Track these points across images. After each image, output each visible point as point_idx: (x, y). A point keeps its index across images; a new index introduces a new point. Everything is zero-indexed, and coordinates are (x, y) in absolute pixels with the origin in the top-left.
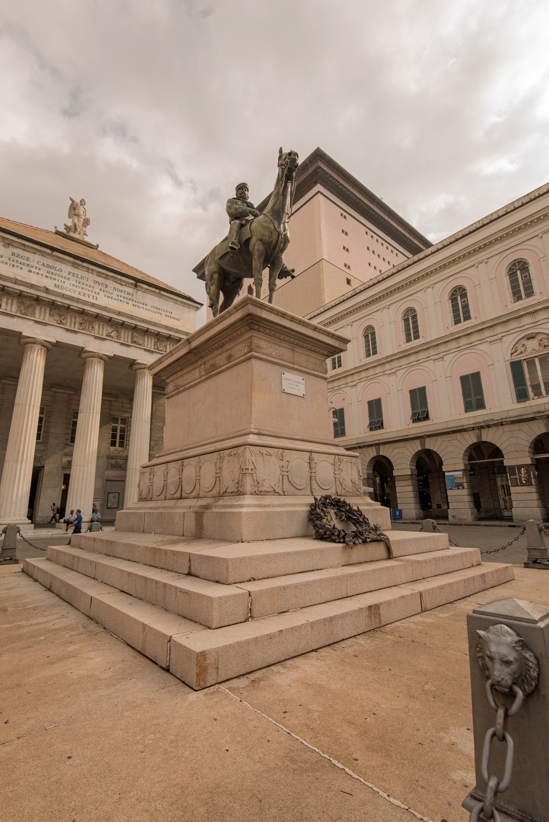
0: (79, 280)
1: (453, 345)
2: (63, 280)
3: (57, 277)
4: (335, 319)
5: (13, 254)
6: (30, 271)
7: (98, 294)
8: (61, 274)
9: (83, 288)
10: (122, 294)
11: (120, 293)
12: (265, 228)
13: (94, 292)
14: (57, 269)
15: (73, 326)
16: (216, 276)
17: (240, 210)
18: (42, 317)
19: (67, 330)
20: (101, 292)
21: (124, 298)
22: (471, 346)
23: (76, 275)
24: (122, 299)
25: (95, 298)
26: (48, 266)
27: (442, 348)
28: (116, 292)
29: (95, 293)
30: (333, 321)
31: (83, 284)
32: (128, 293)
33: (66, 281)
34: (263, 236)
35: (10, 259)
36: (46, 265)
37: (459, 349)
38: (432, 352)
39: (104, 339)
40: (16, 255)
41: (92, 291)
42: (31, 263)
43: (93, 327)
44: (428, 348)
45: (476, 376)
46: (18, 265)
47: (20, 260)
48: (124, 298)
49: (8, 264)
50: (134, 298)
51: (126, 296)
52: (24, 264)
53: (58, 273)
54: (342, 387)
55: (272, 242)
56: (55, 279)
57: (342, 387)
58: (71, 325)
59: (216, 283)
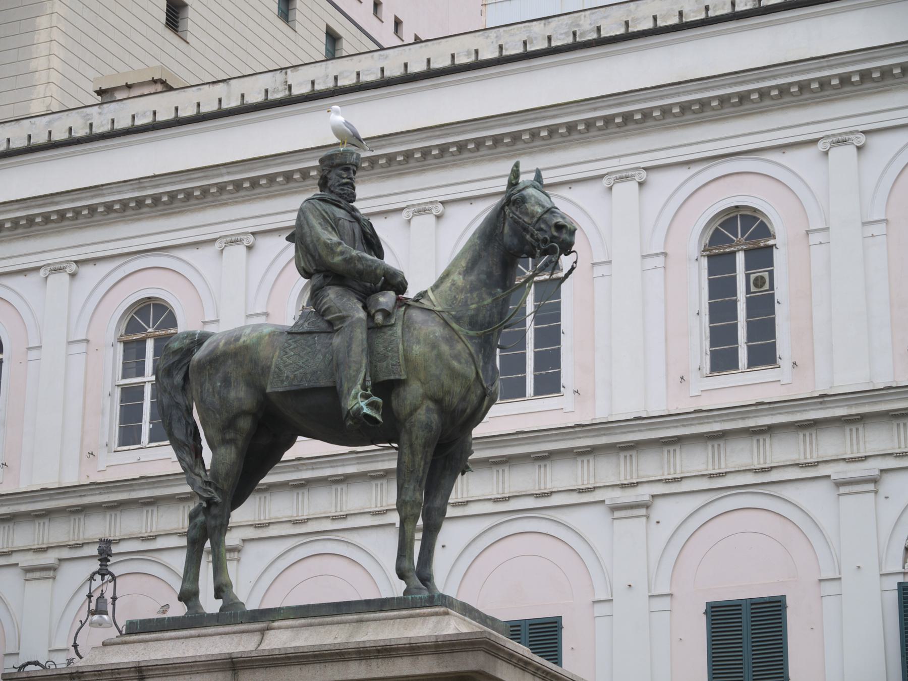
1: (694, 461)
4: (172, 195)
12: (455, 375)
16: (245, 424)
17: (360, 266)
22: (764, 481)
27: (650, 466)
30: (156, 199)
34: (449, 392)
37: (717, 486)
38: (606, 471)
44: (592, 451)
45: (769, 614)
54: (160, 543)
55: (466, 409)
57: (160, 543)
59: (240, 443)
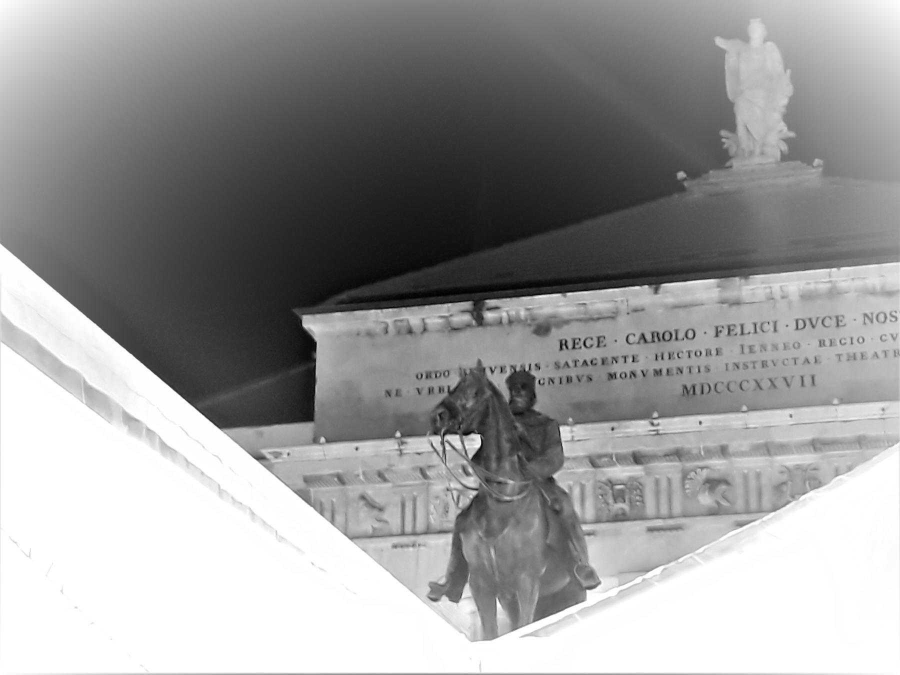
0: (749, 340)
2: (703, 361)
3: (684, 363)
5: (563, 345)
6: (612, 376)
8: (693, 346)
9: (764, 364)
13: (800, 361)
23: (738, 330)
25: (808, 380)
26: (658, 337)
29: (807, 361)
33: (713, 361)
35: (557, 366)
36: (648, 337)
40: (570, 345)
41: (795, 360)
47: (584, 354)
49: (557, 381)
53: (685, 346)
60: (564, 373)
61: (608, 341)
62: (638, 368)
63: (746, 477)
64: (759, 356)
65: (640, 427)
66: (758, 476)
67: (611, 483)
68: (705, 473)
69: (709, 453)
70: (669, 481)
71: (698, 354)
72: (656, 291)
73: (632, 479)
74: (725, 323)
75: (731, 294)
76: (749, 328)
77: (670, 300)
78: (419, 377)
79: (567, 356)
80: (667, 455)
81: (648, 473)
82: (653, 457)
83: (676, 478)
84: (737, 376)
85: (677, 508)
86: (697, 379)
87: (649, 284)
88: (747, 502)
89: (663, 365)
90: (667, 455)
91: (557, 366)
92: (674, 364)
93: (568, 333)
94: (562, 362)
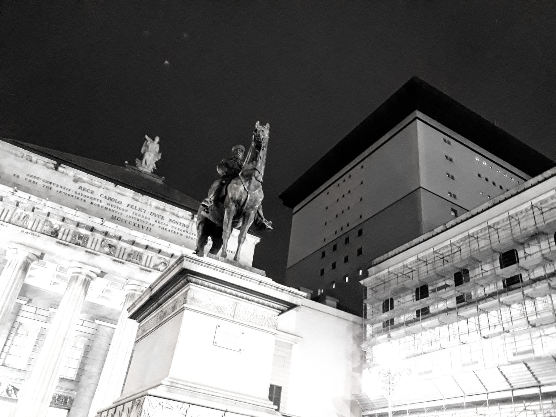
2: (121, 211)
3: (115, 209)
5: (80, 188)
6: (92, 203)
7: (153, 225)
9: (138, 220)
10: (178, 226)
11: (175, 225)
14: (117, 201)
15: (121, 257)
18: (93, 248)
19: (115, 261)
20: (157, 224)
21: (178, 229)
24: (176, 231)
25: (149, 229)
26: (110, 199)
28: (172, 224)
31: (139, 215)
32: (184, 225)
33: (124, 212)
35: (76, 193)
36: (107, 198)
39: (150, 271)
42: (93, 196)
43: (141, 258)
46: (82, 197)
48: (178, 229)
50: (189, 230)
51: (180, 227)
52: (88, 197)
53: (118, 205)
56: (113, 211)
58: (119, 255)
60: (78, 196)
61: (95, 193)
62: (101, 204)
63: (121, 248)
64: (138, 217)
65: (99, 220)
66: (125, 249)
67: (79, 233)
68: (109, 242)
69: (115, 237)
70: (98, 240)
71: (120, 209)
72: (115, 186)
73: (87, 235)
74: (131, 204)
75: (136, 198)
76: (137, 208)
77: (118, 191)
78: (28, 175)
79: (79, 191)
80: (101, 233)
81: (92, 235)
82: (98, 231)
83: (100, 240)
84: (130, 220)
85: (97, 249)
86: (118, 216)
87: (115, 183)
88: (119, 255)
89: (109, 207)
90: (101, 233)
91: (76, 193)
92: (112, 208)
93: (84, 185)
94: (78, 193)
